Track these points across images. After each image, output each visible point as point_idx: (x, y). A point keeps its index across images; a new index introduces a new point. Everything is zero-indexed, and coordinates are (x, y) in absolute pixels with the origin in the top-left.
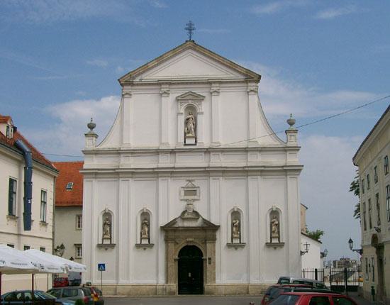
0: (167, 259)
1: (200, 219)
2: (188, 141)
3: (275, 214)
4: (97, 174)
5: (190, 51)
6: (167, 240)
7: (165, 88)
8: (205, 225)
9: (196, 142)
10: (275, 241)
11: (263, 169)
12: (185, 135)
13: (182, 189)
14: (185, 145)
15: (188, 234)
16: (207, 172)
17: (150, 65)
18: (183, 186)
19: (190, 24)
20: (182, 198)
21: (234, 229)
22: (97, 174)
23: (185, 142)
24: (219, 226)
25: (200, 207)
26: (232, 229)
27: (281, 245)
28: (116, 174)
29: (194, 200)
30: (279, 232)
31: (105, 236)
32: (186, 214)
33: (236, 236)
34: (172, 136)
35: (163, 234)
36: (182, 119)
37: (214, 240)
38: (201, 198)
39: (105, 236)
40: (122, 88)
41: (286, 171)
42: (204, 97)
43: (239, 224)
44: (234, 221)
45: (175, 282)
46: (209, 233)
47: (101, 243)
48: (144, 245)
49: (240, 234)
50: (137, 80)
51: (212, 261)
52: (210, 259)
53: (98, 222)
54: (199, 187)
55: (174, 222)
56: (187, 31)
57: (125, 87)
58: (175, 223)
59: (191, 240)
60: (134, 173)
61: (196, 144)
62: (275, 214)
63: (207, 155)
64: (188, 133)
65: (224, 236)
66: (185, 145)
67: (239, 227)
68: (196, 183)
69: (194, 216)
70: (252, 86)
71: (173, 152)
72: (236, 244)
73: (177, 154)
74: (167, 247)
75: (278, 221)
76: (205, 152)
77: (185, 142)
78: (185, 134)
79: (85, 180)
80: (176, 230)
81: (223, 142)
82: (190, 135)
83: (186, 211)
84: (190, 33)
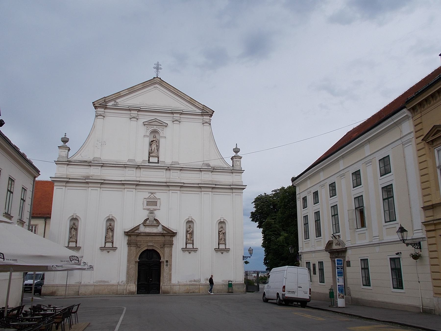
0: (129, 261)
1: (160, 226)
2: (152, 160)
3: (222, 223)
5: (157, 85)
6: (129, 244)
8: (165, 232)
9: (158, 161)
10: (222, 247)
11: (214, 186)
12: (149, 154)
14: (149, 162)
15: (149, 238)
16: (167, 185)
18: (146, 197)
19: (158, 64)
20: (145, 207)
23: (149, 160)
25: (160, 216)
26: (186, 236)
29: (155, 210)
30: (225, 240)
31: (71, 240)
32: (148, 222)
33: (189, 242)
35: (127, 238)
36: (147, 141)
37: (171, 244)
39: (71, 240)
41: (232, 189)
43: (193, 232)
44: (189, 229)
46: (168, 238)
49: (193, 240)
50: (110, 104)
52: (167, 261)
54: (159, 199)
55: (137, 228)
56: (155, 70)
57: (99, 109)
59: (151, 244)
61: (158, 162)
62: (222, 223)
63: (168, 171)
66: (149, 162)
67: (192, 234)
68: (158, 195)
70: (206, 118)
71: (138, 167)
73: (142, 170)
74: (129, 251)
75: (225, 230)
77: (149, 160)
78: (150, 153)
79: (55, 187)
80: (139, 235)
81: (183, 161)
84: (157, 71)
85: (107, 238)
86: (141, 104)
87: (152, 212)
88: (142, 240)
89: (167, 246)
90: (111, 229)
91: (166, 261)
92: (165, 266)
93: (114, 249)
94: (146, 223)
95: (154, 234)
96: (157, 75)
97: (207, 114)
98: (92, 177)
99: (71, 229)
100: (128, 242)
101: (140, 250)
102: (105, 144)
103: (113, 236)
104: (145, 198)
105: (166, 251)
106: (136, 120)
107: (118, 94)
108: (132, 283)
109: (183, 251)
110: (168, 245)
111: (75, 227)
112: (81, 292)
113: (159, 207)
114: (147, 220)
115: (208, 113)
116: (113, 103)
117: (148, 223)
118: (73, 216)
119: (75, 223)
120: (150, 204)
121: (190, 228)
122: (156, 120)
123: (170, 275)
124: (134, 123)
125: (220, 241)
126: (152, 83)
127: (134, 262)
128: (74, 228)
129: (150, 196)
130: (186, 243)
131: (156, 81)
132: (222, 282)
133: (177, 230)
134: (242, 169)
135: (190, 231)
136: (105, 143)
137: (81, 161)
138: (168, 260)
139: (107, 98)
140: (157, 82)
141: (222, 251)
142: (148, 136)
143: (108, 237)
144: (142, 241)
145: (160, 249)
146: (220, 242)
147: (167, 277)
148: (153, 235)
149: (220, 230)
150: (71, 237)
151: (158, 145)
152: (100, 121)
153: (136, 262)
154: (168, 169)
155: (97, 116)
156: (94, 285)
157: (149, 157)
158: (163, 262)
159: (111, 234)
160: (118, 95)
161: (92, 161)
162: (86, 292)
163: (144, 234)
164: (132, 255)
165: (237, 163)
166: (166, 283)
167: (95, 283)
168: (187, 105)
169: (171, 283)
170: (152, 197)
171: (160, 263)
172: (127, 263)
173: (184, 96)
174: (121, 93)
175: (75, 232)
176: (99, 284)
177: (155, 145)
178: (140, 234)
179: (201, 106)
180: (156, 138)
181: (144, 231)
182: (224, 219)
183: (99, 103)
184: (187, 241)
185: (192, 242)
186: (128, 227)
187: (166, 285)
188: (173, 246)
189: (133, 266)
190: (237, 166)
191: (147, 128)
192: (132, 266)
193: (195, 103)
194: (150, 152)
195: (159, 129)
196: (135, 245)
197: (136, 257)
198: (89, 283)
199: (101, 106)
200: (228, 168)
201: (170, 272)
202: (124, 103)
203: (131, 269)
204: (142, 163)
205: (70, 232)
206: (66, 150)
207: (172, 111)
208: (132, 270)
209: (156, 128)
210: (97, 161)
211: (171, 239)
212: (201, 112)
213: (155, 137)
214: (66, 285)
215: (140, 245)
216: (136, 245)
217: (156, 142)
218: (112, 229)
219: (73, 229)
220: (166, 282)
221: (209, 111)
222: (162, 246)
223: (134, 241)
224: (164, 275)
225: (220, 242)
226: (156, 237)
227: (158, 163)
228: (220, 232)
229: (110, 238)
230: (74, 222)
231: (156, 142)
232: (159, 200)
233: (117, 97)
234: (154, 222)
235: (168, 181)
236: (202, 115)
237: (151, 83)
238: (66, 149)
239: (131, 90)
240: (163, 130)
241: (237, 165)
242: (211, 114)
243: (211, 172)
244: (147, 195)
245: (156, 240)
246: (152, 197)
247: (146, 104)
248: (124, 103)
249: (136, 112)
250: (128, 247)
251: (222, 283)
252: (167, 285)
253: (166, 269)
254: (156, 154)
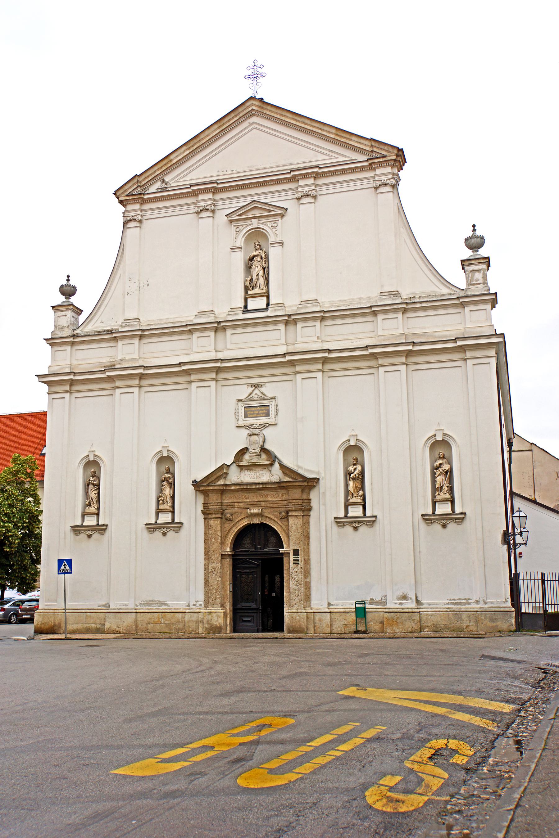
1: (277, 465)
2: (252, 304)
5: (254, 119)
7: (205, 199)
8: (287, 479)
9: (268, 305)
10: (444, 509)
13: (240, 403)
15: (251, 497)
17: (175, 159)
18: (243, 397)
20: (241, 423)
23: (246, 307)
26: (347, 486)
29: (264, 426)
30: (451, 490)
31: (88, 510)
32: (247, 457)
33: (354, 500)
37: (306, 509)
38: (280, 421)
39: (88, 510)
40: (122, 209)
41: (463, 349)
42: (286, 210)
43: (362, 473)
44: (351, 468)
45: (222, 606)
46: (296, 494)
47: (79, 523)
52: (296, 552)
54: (274, 398)
56: (250, 81)
57: (129, 207)
58: (218, 478)
66: (246, 310)
68: (268, 390)
69: (264, 459)
74: (207, 527)
75: (450, 463)
77: (246, 307)
78: (246, 289)
80: (224, 490)
82: (257, 291)
83: (247, 449)
84: (255, 85)
85: (161, 502)
86: (221, 173)
88: (236, 501)
89: (294, 513)
90: (168, 479)
91: (294, 550)
92: (291, 564)
94: (244, 460)
95: (261, 487)
97: (384, 159)
98: (120, 364)
99: (87, 485)
100: (204, 509)
101: (233, 526)
102: (148, 285)
103: (173, 497)
104: (239, 401)
105: (294, 525)
106: (211, 214)
107: (166, 161)
108: (215, 606)
109: (339, 526)
110: (295, 510)
111: (94, 481)
112: (109, 627)
113: (274, 419)
114: (245, 453)
115: (385, 156)
116: (158, 185)
117: (246, 460)
118: (88, 456)
119: (95, 473)
120: (252, 414)
121: (354, 465)
122: (255, 205)
123: (308, 586)
124: (206, 222)
125: (437, 494)
126: (241, 115)
127: (218, 556)
128: (92, 482)
129: (251, 394)
130: (345, 504)
131: (250, 109)
132: (448, 603)
133: (319, 471)
134: (489, 290)
135: (355, 473)
136: (147, 283)
137: (99, 332)
138: (299, 549)
139: (143, 177)
140: (253, 109)
141: (443, 522)
142: (241, 248)
143: (163, 500)
144: (236, 504)
145: (279, 522)
146: (438, 497)
147: (297, 592)
148: (259, 489)
149: (437, 464)
150: (87, 503)
151: (264, 265)
152: (133, 232)
153: (222, 555)
155: (125, 223)
156: (135, 611)
157: (246, 300)
158: (287, 555)
159: (168, 491)
160: (165, 164)
161: (120, 328)
162: (119, 627)
163: (238, 487)
164: (213, 540)
165: (475, 278)
166: (295, 606)
167: (139, 607)
168: (331, 151)
169: (310, 606)
170: (256, 394)
172: (205, 559)
173: (320, 129)
174: (172, 157)
175: (96, 492)
176: (147, 607)
177: (259, 267)
178: (228, 488)
179: (367, 143)
180: (261, 249)
181: (239, 481)
182: (444, 434)
183: (126, 193)
184: (349, 498)
185: (360, 501)
187: (295, 611)
188: (312, 513)
189: (217, 565)
190: (474, 284)
191: (238, 230)
192: (215, 565)
193: (351, 140)
194: (248, 287)
195: (266, 226)
196: (220, 516)
197: (222, 543)
198: (125, 607)
199: (131, 198)
200: (450, 294)
201: (305, 578)
202: (183, 180)
203: (212, 572)
204: (228, 316)
205: (87, 493)
206: (66, 312)
207: (293, 173)
208: (214, 575)
209: (258, 223)
210: (129, 325)
211: (305, 497)
212: (368, 160)
213: (258, 247)
214: (64, 611)
215: (232, 515)
216: (222, 514)
217: (262, 258)
218: (170, 481)
219: (91, 487)
220: (296, 604)
221: (388, 151)
222: (283, 514)
223: (215, 504)
224: (291, 586)
225: (438, 497)
226: (267, 493)
227: (266, 309)
228: (436, 469)
229: (167, 501)
230: (93, 470)
231: (262, 258)
232: (273, 400)
233: (164, 168)
234: (260, 455)
235: (291, 349)
237: (238, 117)
238: (67, 310)
239: (193, 146)
240: (275, 225)
241: (474, 282)
242: (394, 157)
243: (403, 313)
245: (269, 499)
246: (256, 396)
247: (232, 171)
248: (183, 180)
249: (210, 196)
250: (205, 522)
251: (447, 606)
252: (299, 611)
253: (293, 572)
254: (262, 288)
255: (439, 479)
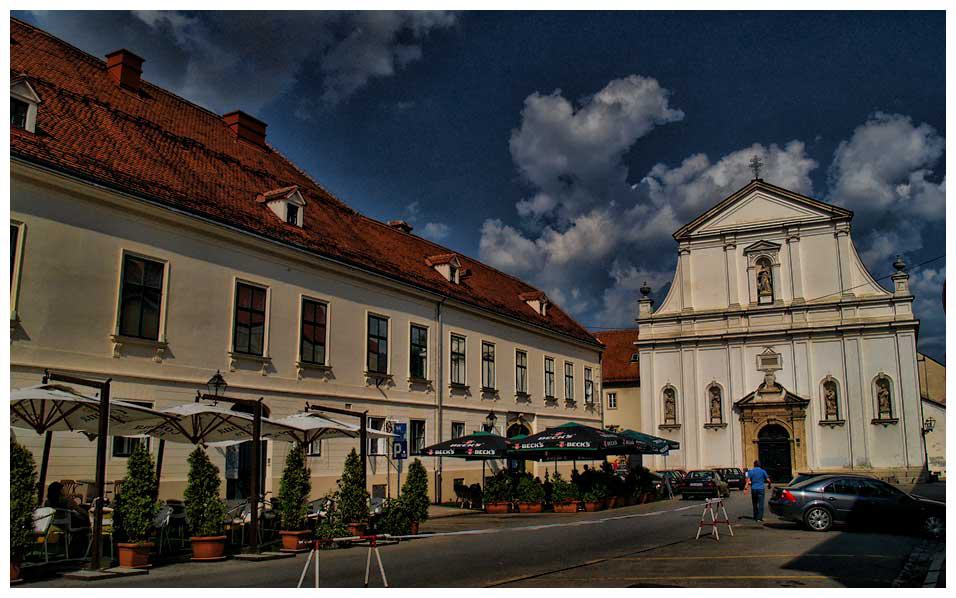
1: (784, 392)
2: (763, 300)
3: (883, 382)
4: (654, 345)
7: (729, 239)
9: (773, 299)
10: (885, 416)
12: (759, 293)
14: (759, 304)
16: (789, 336)
17: (709, 215)
21: (829, 403)
22: (654, 345)
24: (808, 401)
25: (783, 378)
27: (894, 422)
28: (677, 343)
29: (775, 370)
34: (744, 296)
36: (754, 274)
42: (780, 245)
43: (836, 396)
47: (663, 423)
48: (715, 425)
51: (802, 442)
52: (798, 440)
53: (659, 398)
55: (751, 396)
59: (772, 417)
60: (698, 342)
62: (883, 382)
64: (764, 289)
65: (816, 412)
68: (777, 350)
69: (775, 389)
71: (745, 314)
72: (833, 420)
76: (785, 312)
78: (759, 291)
80: (753, 407)
81: (808, 295)
82: (765, 292)
87: (769, 373)
93: (723, 426)
96: (757, 175)
103: (720, 409)
154: (789, 311)
159: (717, 406)
171: (789, 442)
186: (738, 397)
195: (770, 255)
205: (666, 407)
227: (772, 303)
236: (833, 222)
244: (761, 351)
255: (882, 400)
